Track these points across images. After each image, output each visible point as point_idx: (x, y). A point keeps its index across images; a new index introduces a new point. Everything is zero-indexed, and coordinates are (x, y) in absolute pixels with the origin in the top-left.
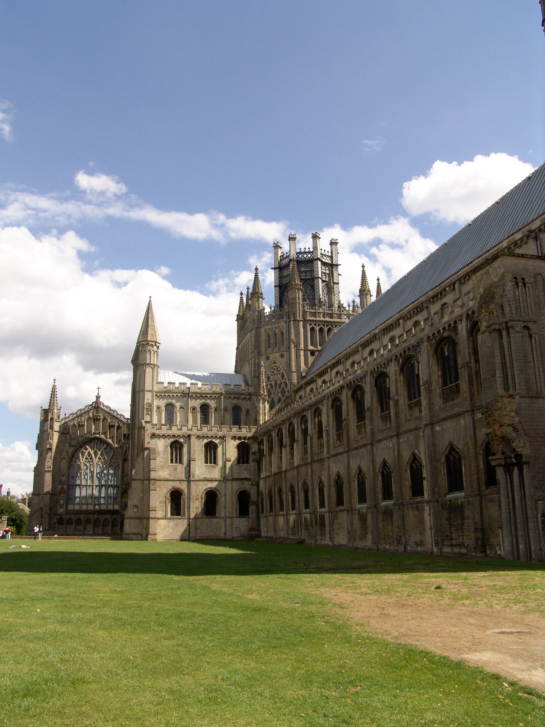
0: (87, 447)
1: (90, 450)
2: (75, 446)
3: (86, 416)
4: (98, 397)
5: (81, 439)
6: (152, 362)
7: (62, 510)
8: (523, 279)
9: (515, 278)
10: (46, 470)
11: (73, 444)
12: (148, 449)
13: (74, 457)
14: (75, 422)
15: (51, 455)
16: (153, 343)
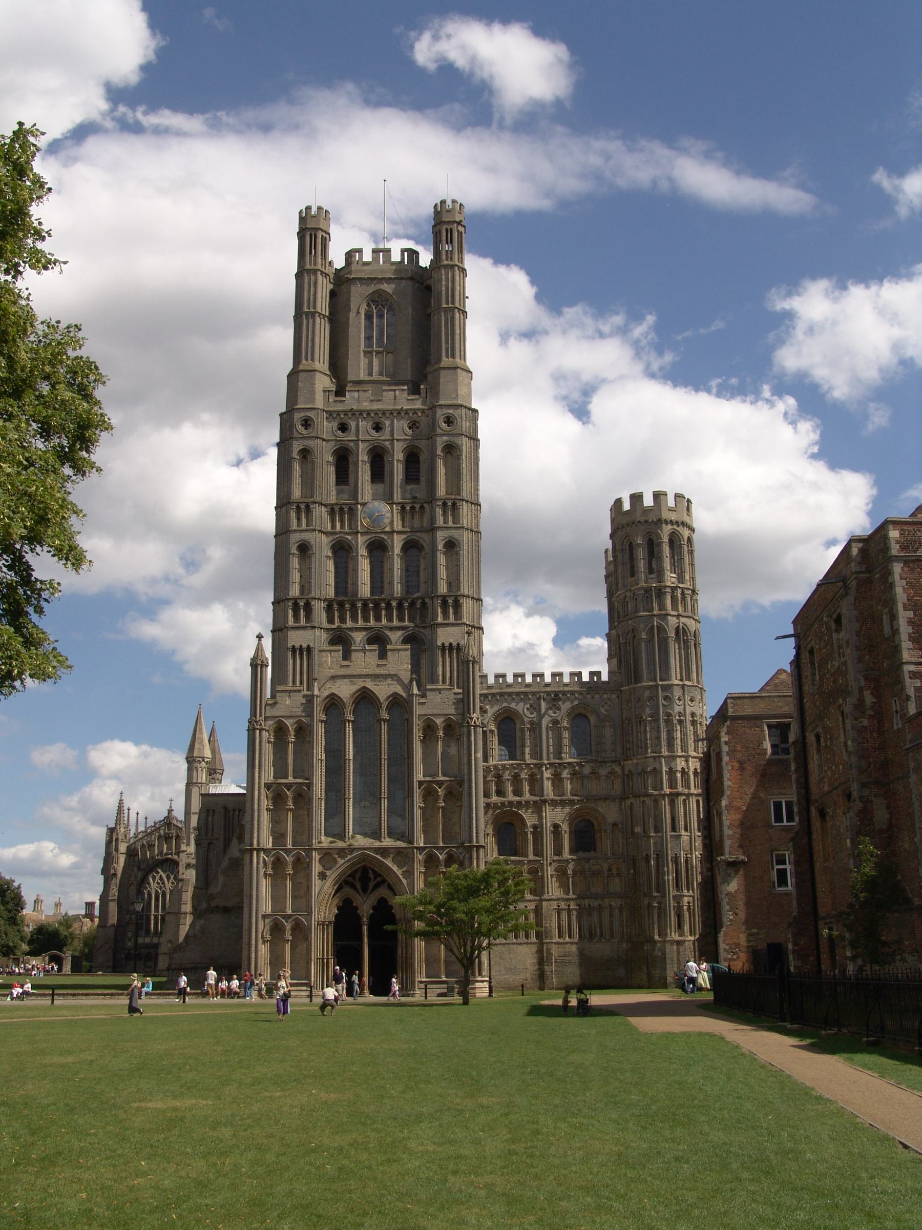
0: (159, 870)
1: (162, 873)
2: (144, 870)
3: (157, 834)
4: (170, 811)
5: (151, 862)
6: (199, 781)
7: (130, 944)
8: (214, 810)
9: (208, 810)
10: (110, 898)
11: (142, 867)
12: (182, 880)
13: (144, 881)
14: (145, 842)
15: (116, 881)
16: (201, 759)
